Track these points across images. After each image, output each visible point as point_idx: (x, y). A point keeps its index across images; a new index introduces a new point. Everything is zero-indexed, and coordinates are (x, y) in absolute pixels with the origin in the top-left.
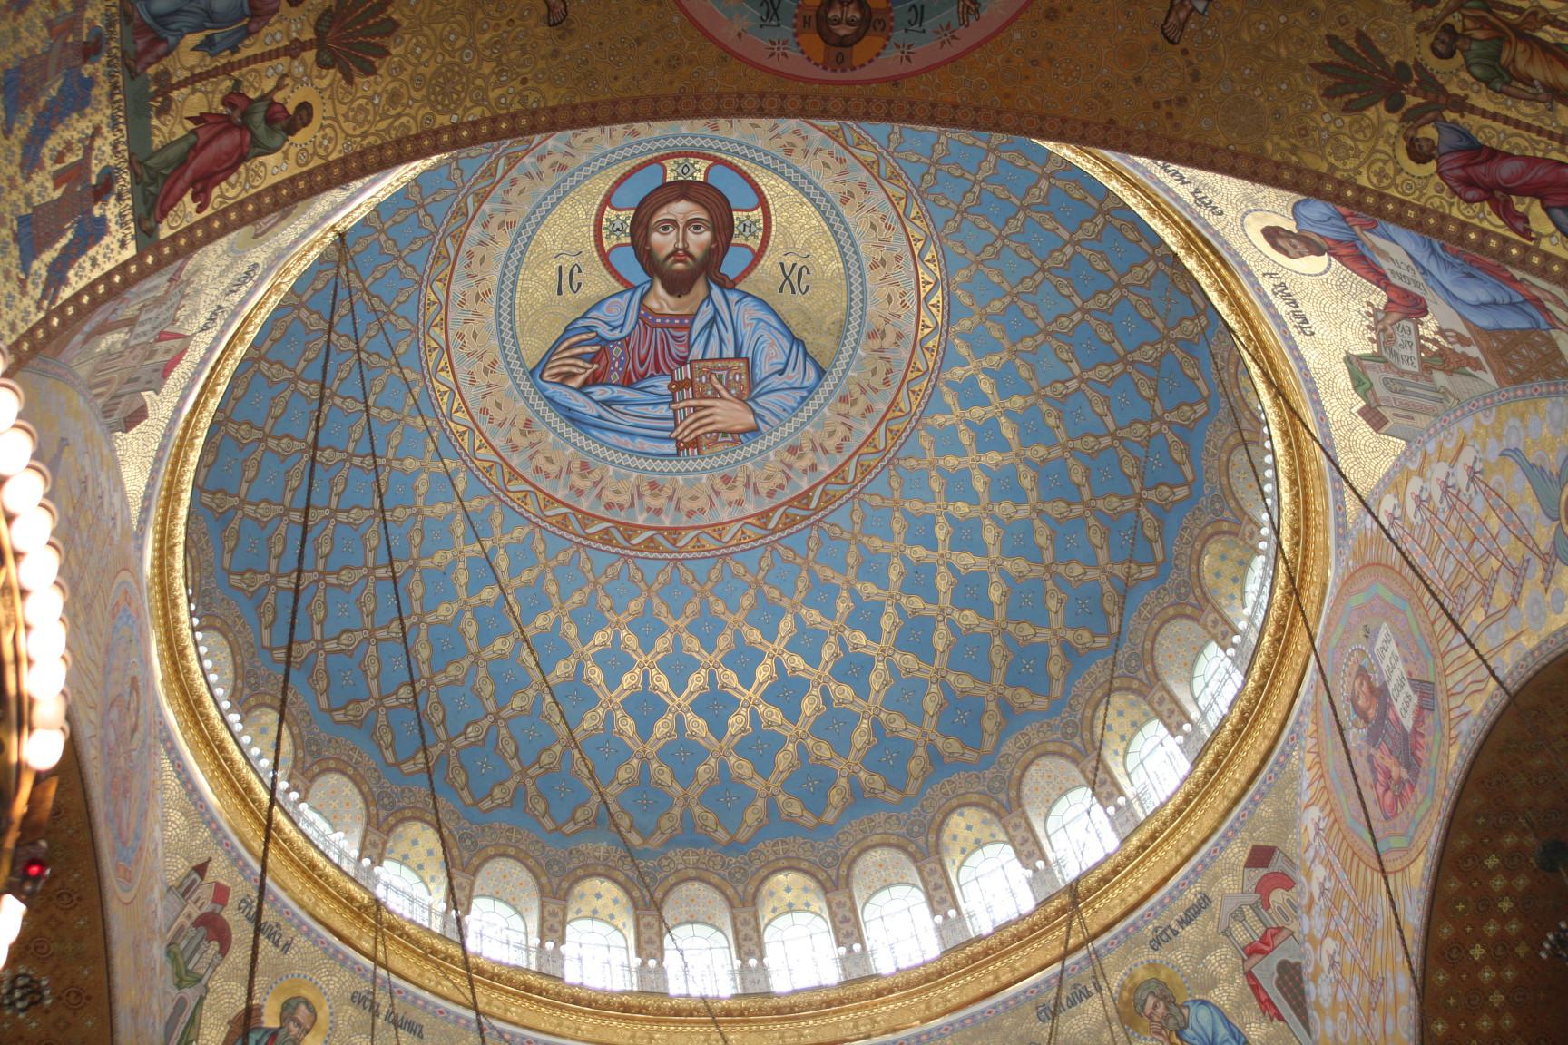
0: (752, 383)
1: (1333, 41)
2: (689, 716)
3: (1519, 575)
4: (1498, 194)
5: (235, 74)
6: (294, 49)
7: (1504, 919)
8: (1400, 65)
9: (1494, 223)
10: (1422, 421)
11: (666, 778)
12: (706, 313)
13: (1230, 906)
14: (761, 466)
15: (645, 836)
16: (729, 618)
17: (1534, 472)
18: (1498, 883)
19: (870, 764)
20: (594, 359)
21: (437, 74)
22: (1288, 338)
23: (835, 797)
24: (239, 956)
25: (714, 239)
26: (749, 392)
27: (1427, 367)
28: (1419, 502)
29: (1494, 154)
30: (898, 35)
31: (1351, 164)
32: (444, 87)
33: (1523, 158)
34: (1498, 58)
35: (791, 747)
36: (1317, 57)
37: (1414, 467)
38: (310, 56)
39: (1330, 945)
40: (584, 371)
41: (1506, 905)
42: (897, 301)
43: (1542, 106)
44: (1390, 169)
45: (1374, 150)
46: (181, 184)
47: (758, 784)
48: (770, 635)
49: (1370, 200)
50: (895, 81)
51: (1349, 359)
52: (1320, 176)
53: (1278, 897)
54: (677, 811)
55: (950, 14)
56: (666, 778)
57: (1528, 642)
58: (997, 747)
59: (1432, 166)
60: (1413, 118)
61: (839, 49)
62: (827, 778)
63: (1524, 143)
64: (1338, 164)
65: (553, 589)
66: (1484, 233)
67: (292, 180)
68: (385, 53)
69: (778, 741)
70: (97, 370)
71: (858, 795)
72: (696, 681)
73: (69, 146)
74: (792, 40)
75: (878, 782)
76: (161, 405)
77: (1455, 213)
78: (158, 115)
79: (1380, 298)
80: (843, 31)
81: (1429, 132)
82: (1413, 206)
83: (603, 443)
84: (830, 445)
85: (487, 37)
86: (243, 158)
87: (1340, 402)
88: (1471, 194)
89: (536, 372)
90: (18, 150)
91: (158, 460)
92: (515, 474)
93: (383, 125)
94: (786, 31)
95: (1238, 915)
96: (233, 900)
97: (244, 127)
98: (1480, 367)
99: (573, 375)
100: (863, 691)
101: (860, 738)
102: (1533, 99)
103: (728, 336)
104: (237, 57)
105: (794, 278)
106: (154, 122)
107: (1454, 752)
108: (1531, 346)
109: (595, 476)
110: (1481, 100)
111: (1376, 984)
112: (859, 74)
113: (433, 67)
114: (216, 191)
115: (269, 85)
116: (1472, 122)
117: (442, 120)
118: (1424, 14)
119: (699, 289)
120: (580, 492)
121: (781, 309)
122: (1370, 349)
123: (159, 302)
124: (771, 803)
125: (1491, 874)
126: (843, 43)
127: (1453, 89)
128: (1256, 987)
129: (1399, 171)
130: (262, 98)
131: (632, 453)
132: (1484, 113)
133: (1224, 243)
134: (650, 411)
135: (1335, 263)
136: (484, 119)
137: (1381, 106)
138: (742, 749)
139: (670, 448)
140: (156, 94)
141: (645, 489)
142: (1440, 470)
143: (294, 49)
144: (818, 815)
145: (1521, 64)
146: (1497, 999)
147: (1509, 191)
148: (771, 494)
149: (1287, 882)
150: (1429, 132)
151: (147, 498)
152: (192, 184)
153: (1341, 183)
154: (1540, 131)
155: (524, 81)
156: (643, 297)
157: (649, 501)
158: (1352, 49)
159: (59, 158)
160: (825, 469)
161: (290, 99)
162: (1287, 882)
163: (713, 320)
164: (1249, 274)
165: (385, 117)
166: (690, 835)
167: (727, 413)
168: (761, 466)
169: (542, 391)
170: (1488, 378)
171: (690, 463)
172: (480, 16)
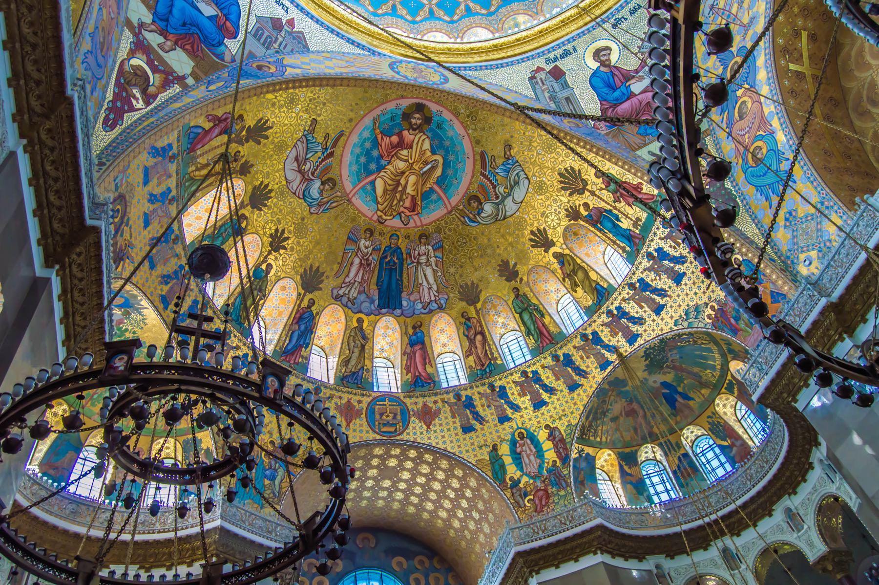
1: (267, 138)
6: (593, 193)
8: (247, 141)
21: (552, 153)
30: (400, 113)
36: (271, 131)
38: (589, 187)
46: (645, 197)
50: (402, 97)
60: (243, 128)
61: (420, 108)
67: (609, 161)
73: (671, 246)
78: (641, 220)
80: (417, 116)
90: (686, 265)
94: (435, 119)
113: (552, 155)
114: (635, 183)
115: (603, 191)
118: (244, 159)
130: (609, 191)
143: (593, 193)
147: (215, 125)
152: (640, 192)
159: (675, 248)
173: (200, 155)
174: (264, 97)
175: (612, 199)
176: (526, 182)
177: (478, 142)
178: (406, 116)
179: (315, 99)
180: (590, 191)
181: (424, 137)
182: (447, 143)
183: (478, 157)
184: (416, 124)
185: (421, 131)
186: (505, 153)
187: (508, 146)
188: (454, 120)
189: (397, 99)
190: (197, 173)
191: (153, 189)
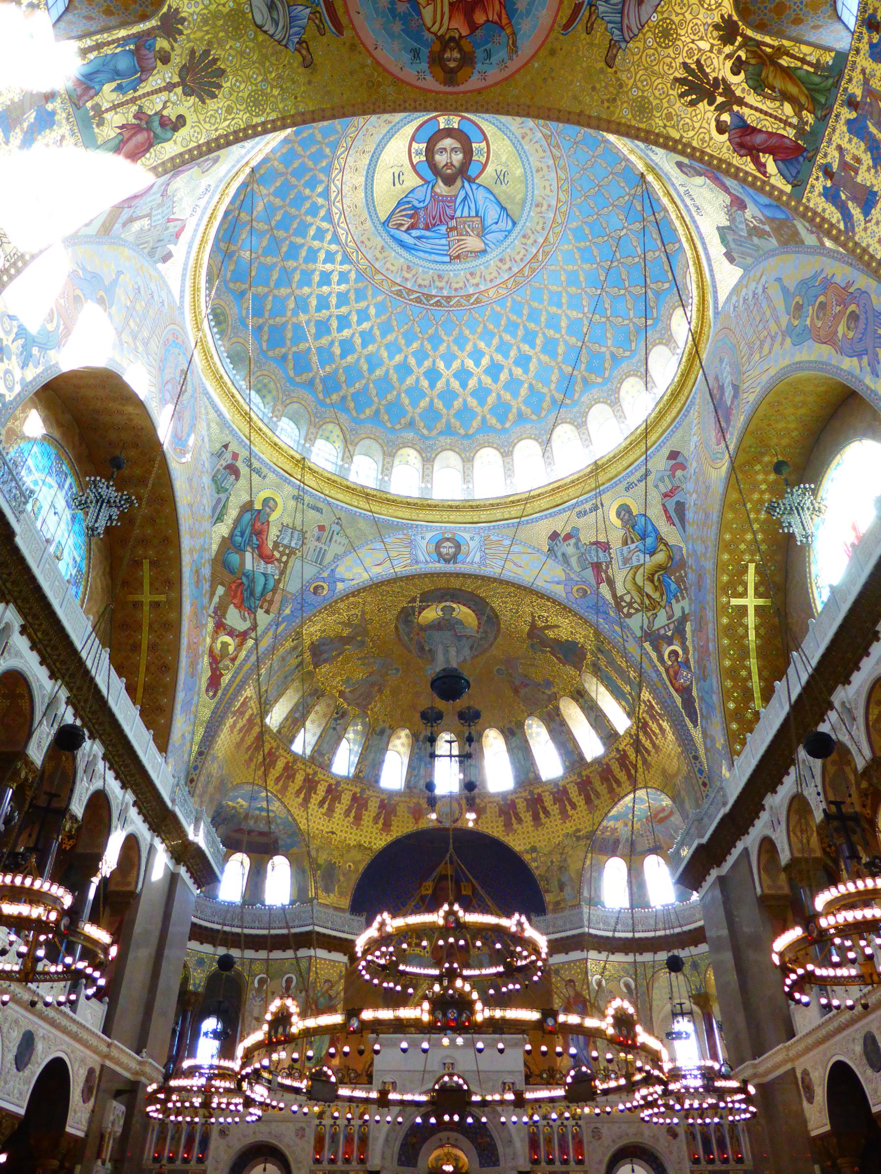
0: (484, 228)
1: (685, 64)
2: (452, 380)
3: (773, 339)
4: (754, 152)
5: (138, 102)
7: (763, 492)
8: (716, 79)
9: (751, 167)
10: (749, 260)
11: (441, 406)
12: (462, 195)
13: (659, 475)
14: (487, 268)
15: (430, 430)
16: (471, 337)
17: (785, 290)
18: (760, 477)
19: (526, 402)
20: (411, 216)
21: (249, 96)
22: (692, 217)
23: (511, 417)
24: (243, 482)
25: (464, 158)
26: (482, 233)
27: (750, 235)
28: (745, 300)
29: (754, 130)
30: (479, 66)
31: (691, 133)
32: (256, 102)
33: (767, 132)
34: (760, 75)
35: (494, 394)
36: (679, 76)
37: (745, 283)
38: (179, 90)
39: (694, 496)
40: (408, 222)
41: (763, 487)
42: (548, 188)
43: (778, 104)
44: (707, 139)
45: (702, 123)
47: (479, 410)
48: (488, 345)
49: (698, 154)
50: (479, 91)
51: (718, 228)
52: (676, 142)
53: (679, 473)
54: (444, 420)
55: (503, 54)
56: (441, 406)
57: (772, 372)
58: (580, 397)
59: (727, 135)
60: (721, 108)
62: (507, 408)
63: (768, 124)
64: (685, 135)
65: (395, 323)
66: (747, 173)
67: (181, 154)
68: (219, 87)
69: (488, 391)
70: (138, 238)
71: (520, 415)
72: (456, 365)
74: (428, 71)
75: (529, 411)
76: (179, 250)
77: (735, 162)
78: (98, 125)
79: (728, 200)
80: (452, 65)
81: (726, 117)
82: (716, 158)
83: (417, 257)
84: (518, 258)
85: (273, 75)
86: (151, 145)
87: (717, 249)
88: (743, 152)
89: (386, 223)
91: (184, 275)
92: (378, 271)
93: (227, 123)
94: (424, 66)
95: (662, 479)
96: (240, 459)
97: (149, 129)
98: (769, 236)
99: (402, 225)
100: (526, 371)
101: (524, 392)
102: (774, 99)
103: (473, 206)
104: (137, 94)
105: (501, 177)
106: (96, 130)
107: (742, 418)
108: (788, 227)
109: (413, 272)
110: (752, 99)
111: (707, 515)
112: (462, 88)
115: (159, 107)
116: (746, 111)
117: (256, 120)
118: (728, 49)
119: (459, 183)
120: (407, 280)
121: (496, 191)
122: (728, 223)
123: (160, 206)
124: (484, 418)
125: (757, 473)
126: (453, 71)
127: (738, 93)
128: (666, 511)
129: (711, 139)
130: (156, 114)
131: (430, 261)
132: (751, 107)
133: (661, 169)
134: (437, 241)
135: (708, 181)
136: (278, 119)
137: (706, 101)
138: (473, 394)
139: (447, 259)
140: (94, 117)
141: (436, 278)
142: (753, 285)
144: (503, 423)
145: (770, 79)
146: (756, 526)
147: (759, 151)
148: (491, 281)
149: (683, 467)
150: (726, 117)
151: (182, 291)
153: (686, 145)
154: (776, 118)
155: (296, 98)
156: (433, 187)
157: (438, 284)
158: (693, 70)
160: (515, 270)
161: (171, 113)
162: (683, 467)
163: (465, 198)
164: (673, 185)
165: (225, 120)
166: (449, 430)
167: (473, 242)
168: (487, 268)
169: (389, 232)
170: (774, 242)
171: (457, 266)
172: (268, 64)
173: (790, 125)
174: (682, 137)
175: (145, 110)
176: (259, 22)
177: (353, 47)
178: (467, 60)
179: (608, 100)
180: (174, 86)
181: (435, 29)
182: (398, 27)
183: (344, 20)
184: (452, 50)
185: (440, 38)
186: (308, 50)
187: (308, 64)
188: (396, 71)
189: (485, 88)
190: (803, 100)
191: (868, 170)
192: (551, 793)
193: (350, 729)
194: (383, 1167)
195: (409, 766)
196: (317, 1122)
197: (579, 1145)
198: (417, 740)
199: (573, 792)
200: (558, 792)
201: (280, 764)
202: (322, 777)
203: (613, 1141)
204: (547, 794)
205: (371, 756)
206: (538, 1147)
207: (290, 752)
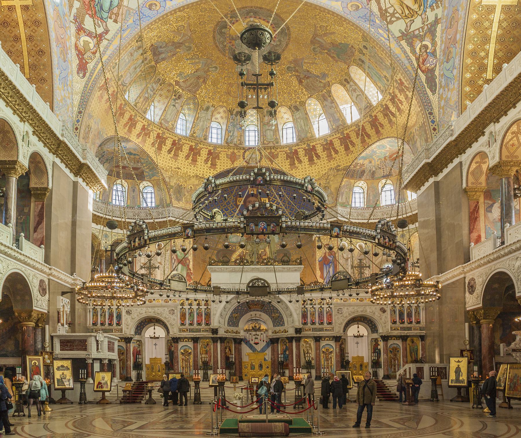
192: (322, 145)
193: (185, 107)
194: (219, 327)
195: (227, 130)
196: (181, 307)
197: (330, 315)
198: (232, 114)
199: (337, 144)
200: (326, 144)
201: (139, 126)
202: (168, 135)
203: (349, 314)
204: (319, 145)
205: (201, 123)
206: (307, 317)
207: (145, 119)
